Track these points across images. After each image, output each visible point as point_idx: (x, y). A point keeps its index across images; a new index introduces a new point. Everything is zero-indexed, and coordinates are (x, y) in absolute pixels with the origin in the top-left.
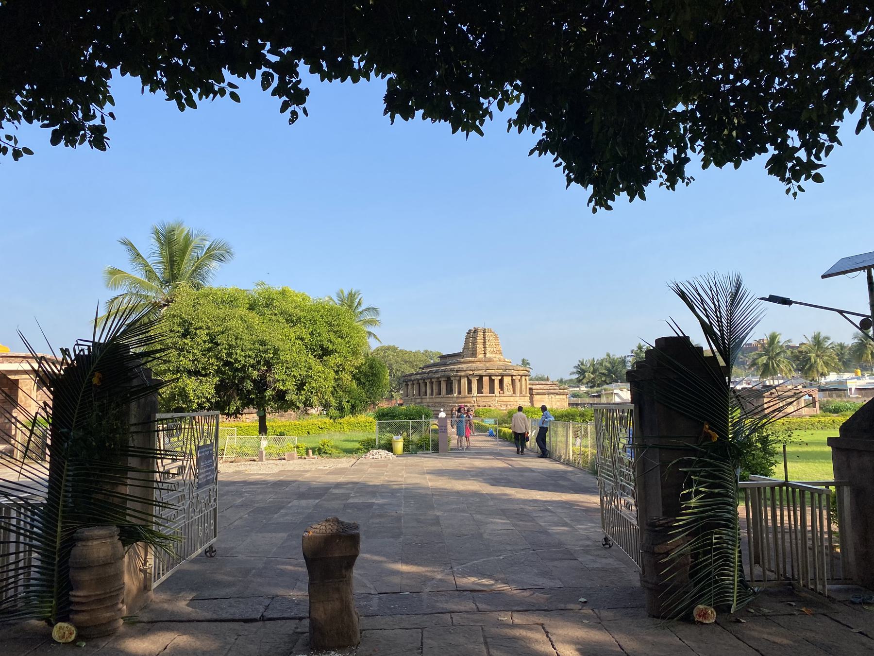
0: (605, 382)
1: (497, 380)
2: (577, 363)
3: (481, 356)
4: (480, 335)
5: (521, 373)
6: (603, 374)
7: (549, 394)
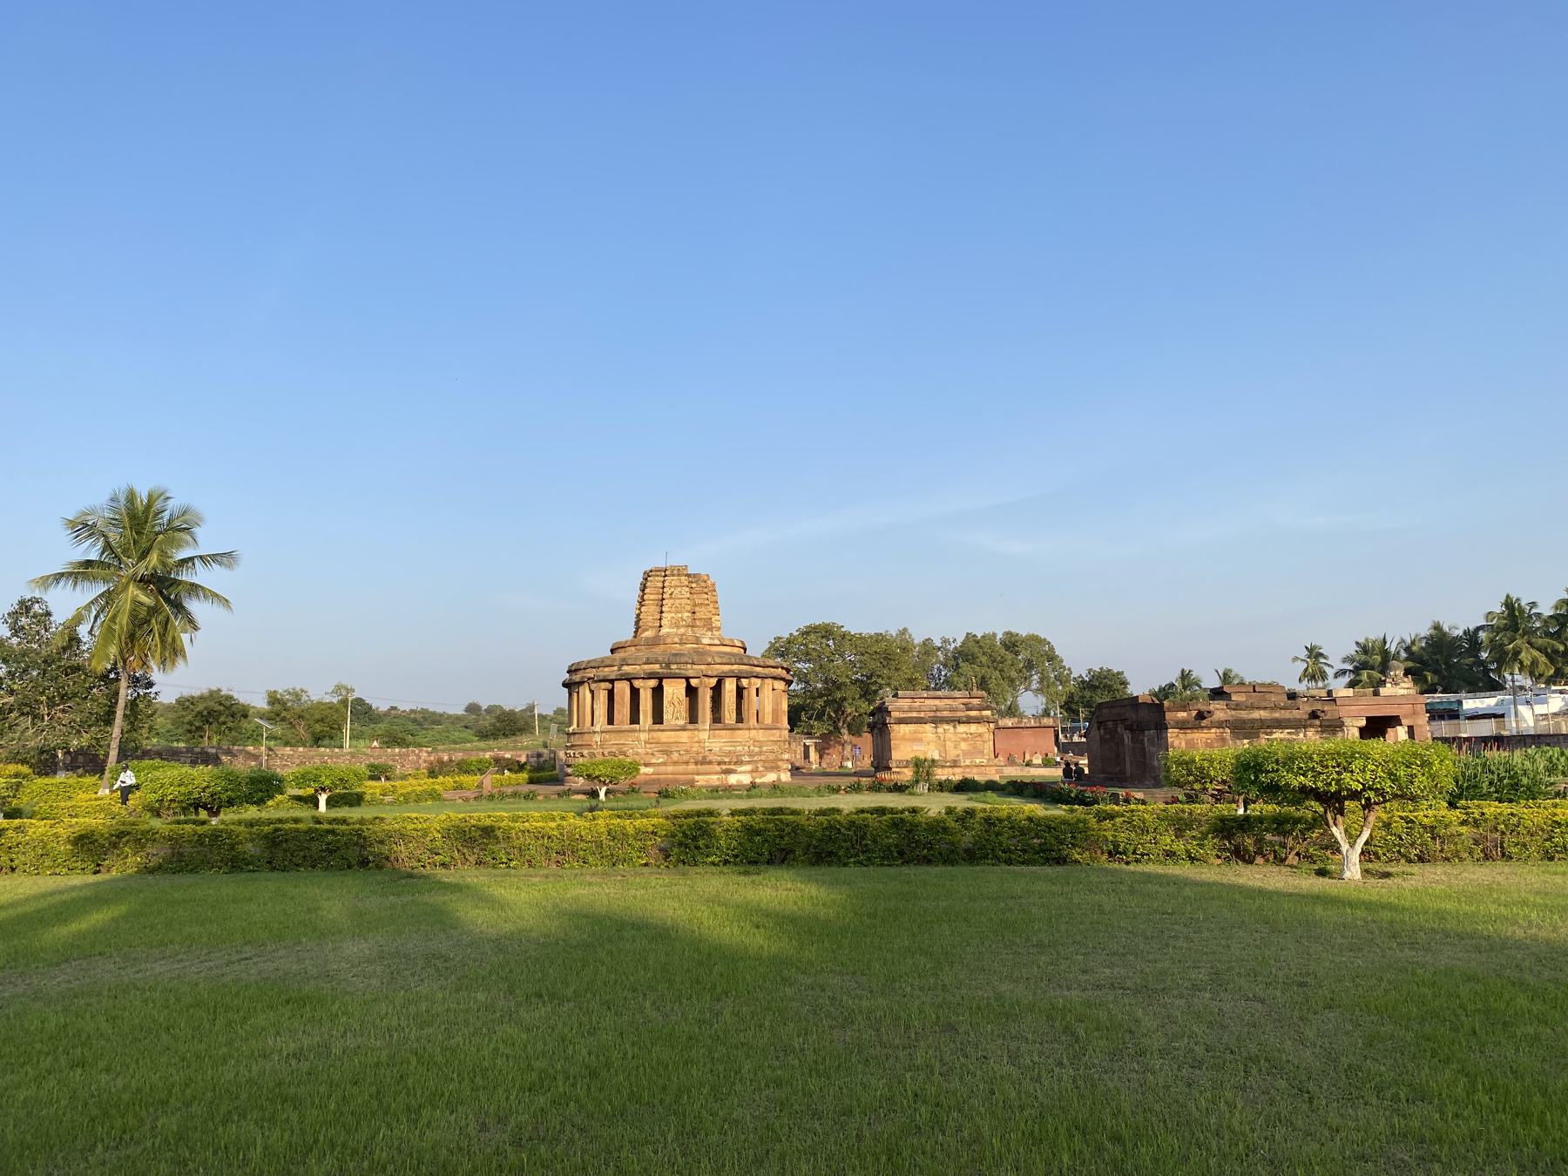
1: (646, 689)
2: (1352, 650)
4: (655, 582)
7: (936, 721)
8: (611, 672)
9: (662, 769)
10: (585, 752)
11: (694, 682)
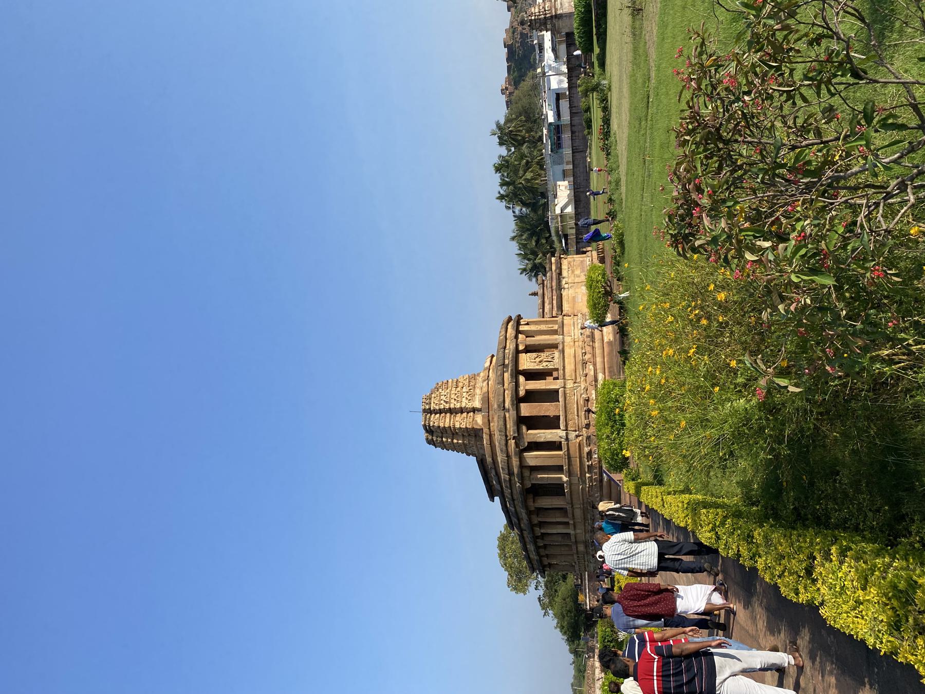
0: (548, 239)
1: (525, 385)
3: (479, 419)
4: (436, 421)
5: (511, 331)
6: (537, 242)
7: (560, 288)
8: (511, 417)
9: (599, 366)
10: (586, 449)
11: (521, 348)
